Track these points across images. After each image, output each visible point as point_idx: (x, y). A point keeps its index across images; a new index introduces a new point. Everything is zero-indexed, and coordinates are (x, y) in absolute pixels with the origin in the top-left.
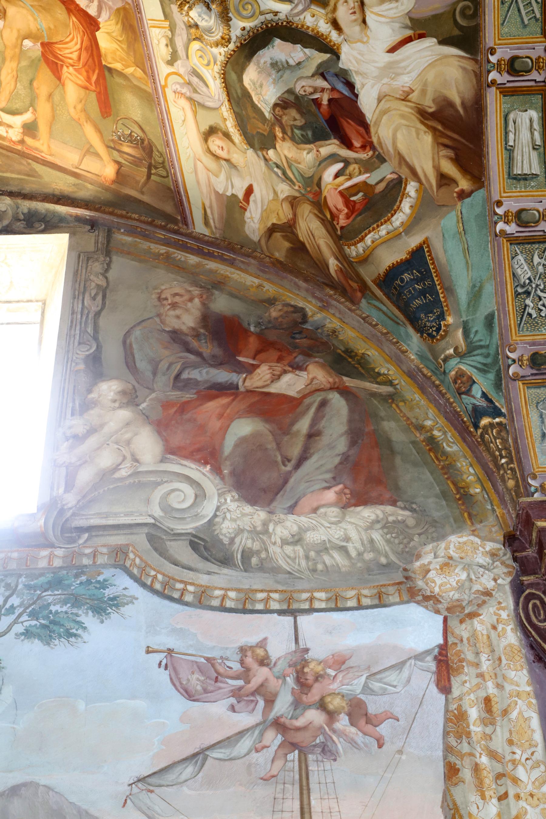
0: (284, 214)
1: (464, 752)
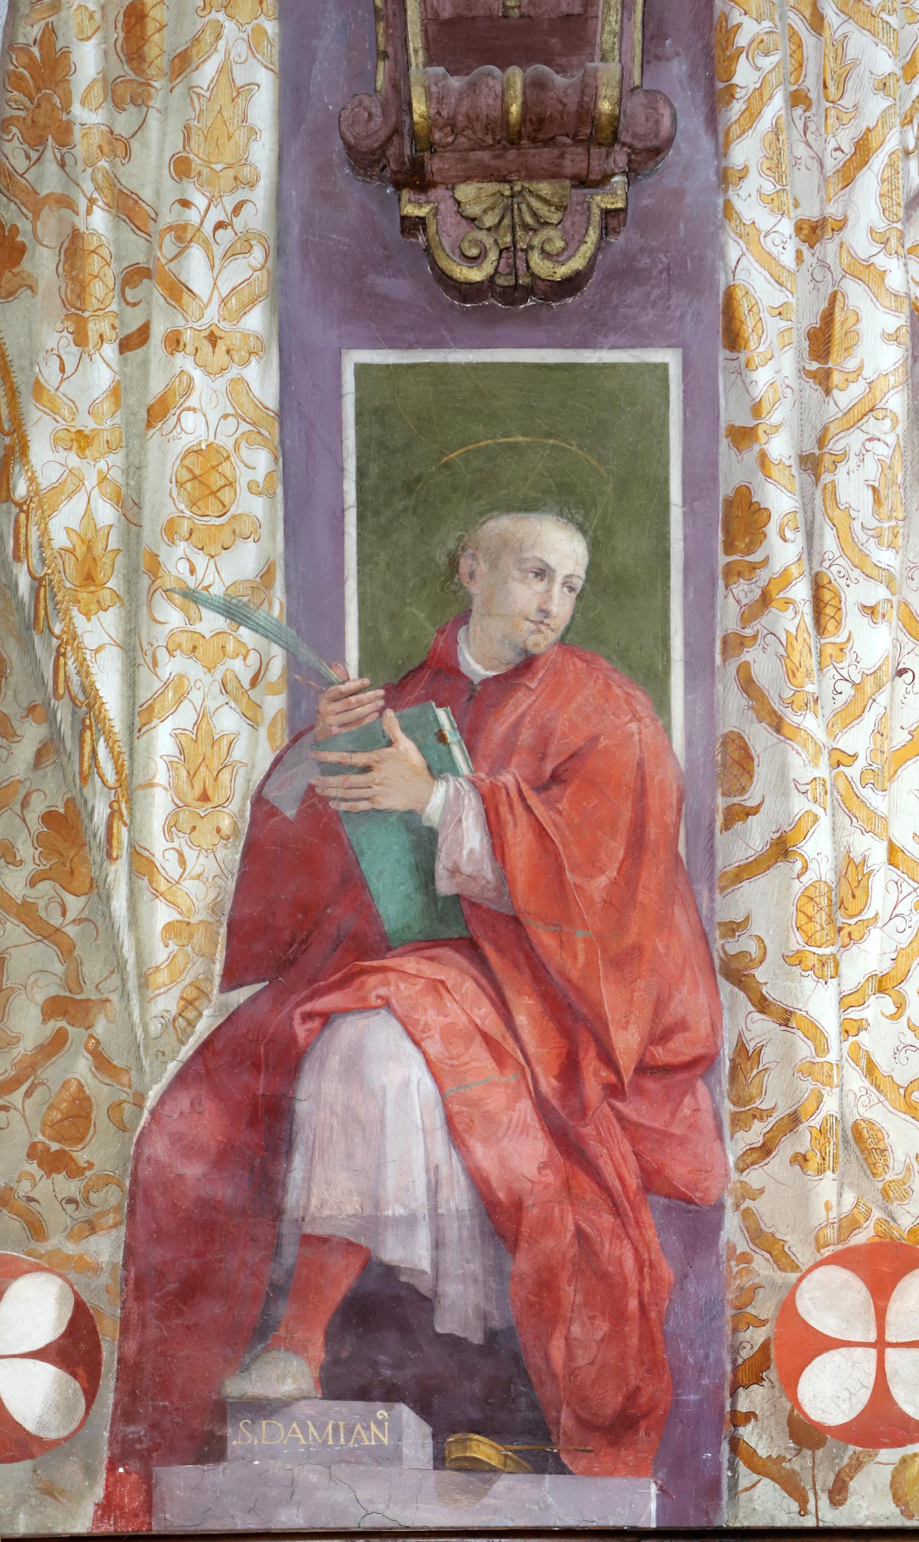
1: (44, 192)
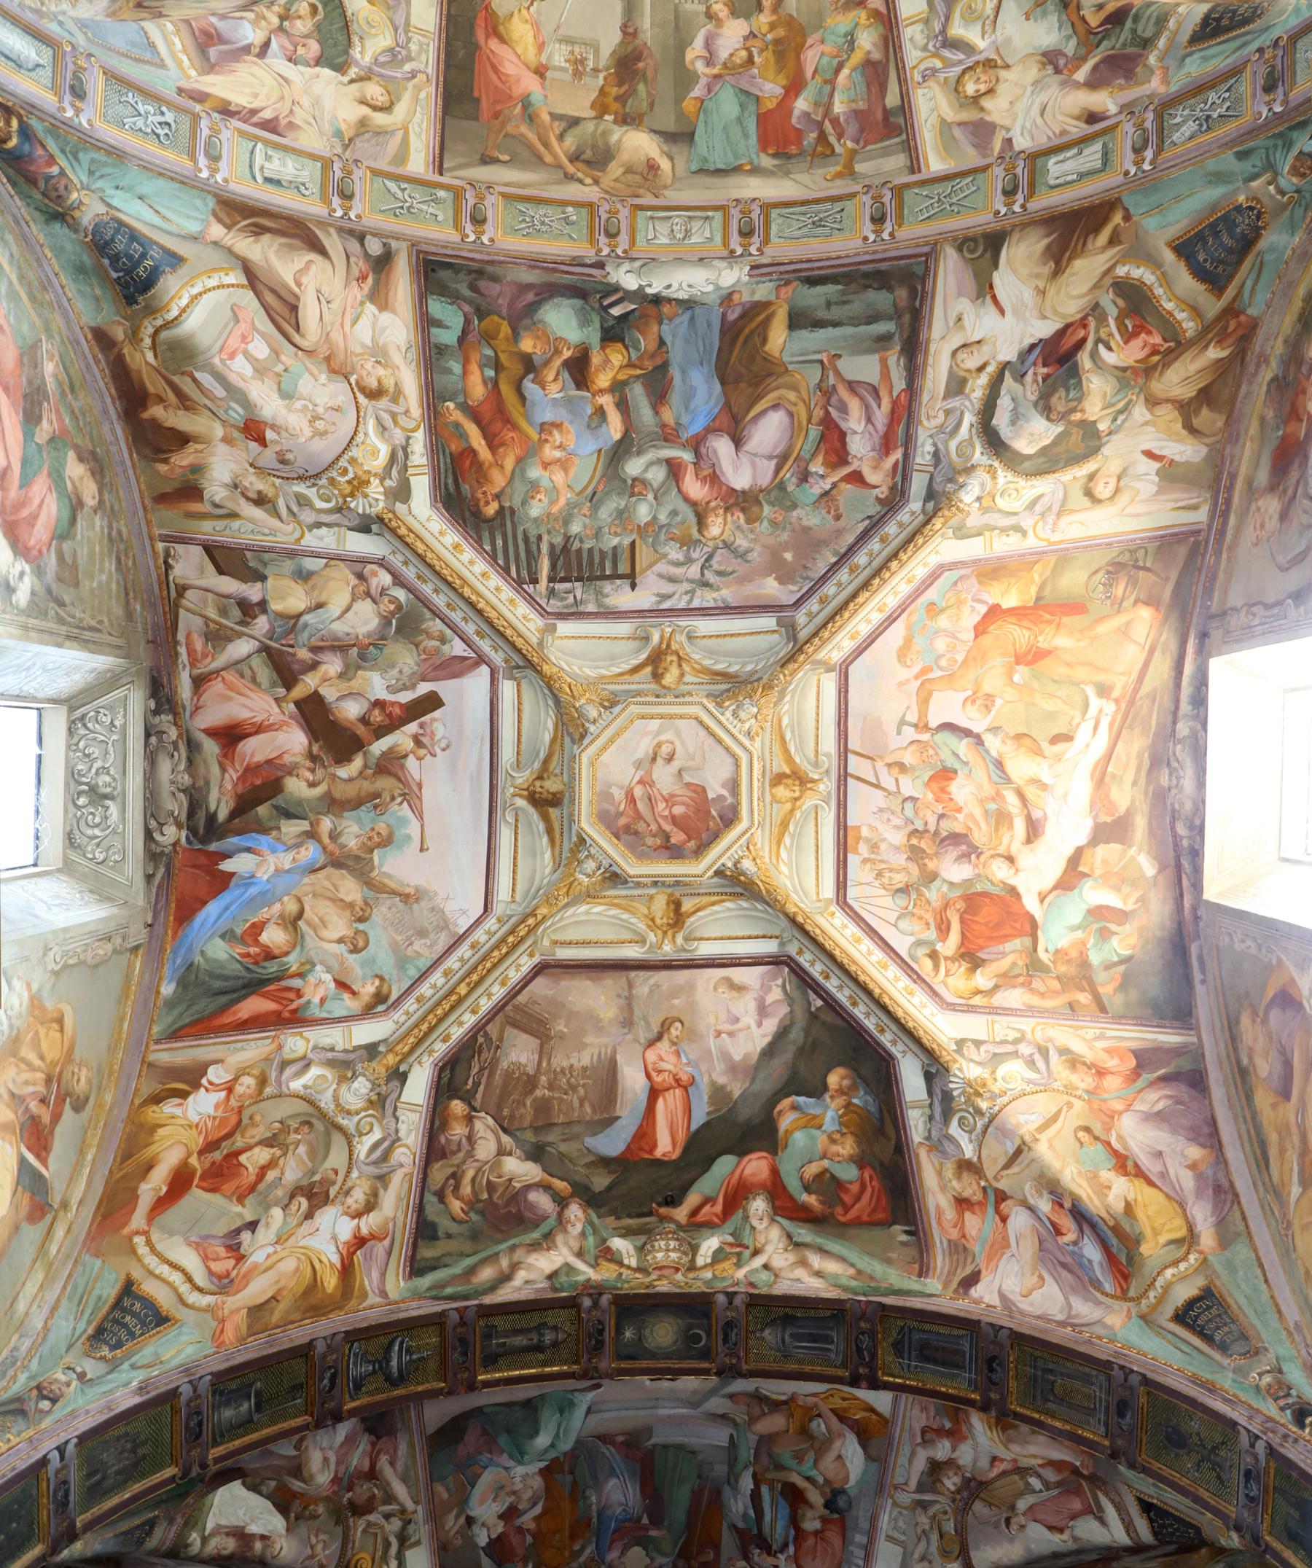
0: (1168, 414)
